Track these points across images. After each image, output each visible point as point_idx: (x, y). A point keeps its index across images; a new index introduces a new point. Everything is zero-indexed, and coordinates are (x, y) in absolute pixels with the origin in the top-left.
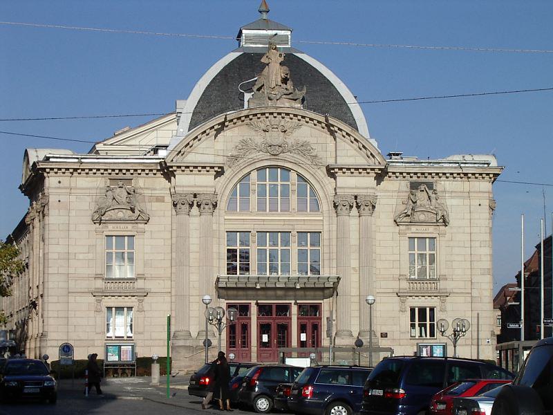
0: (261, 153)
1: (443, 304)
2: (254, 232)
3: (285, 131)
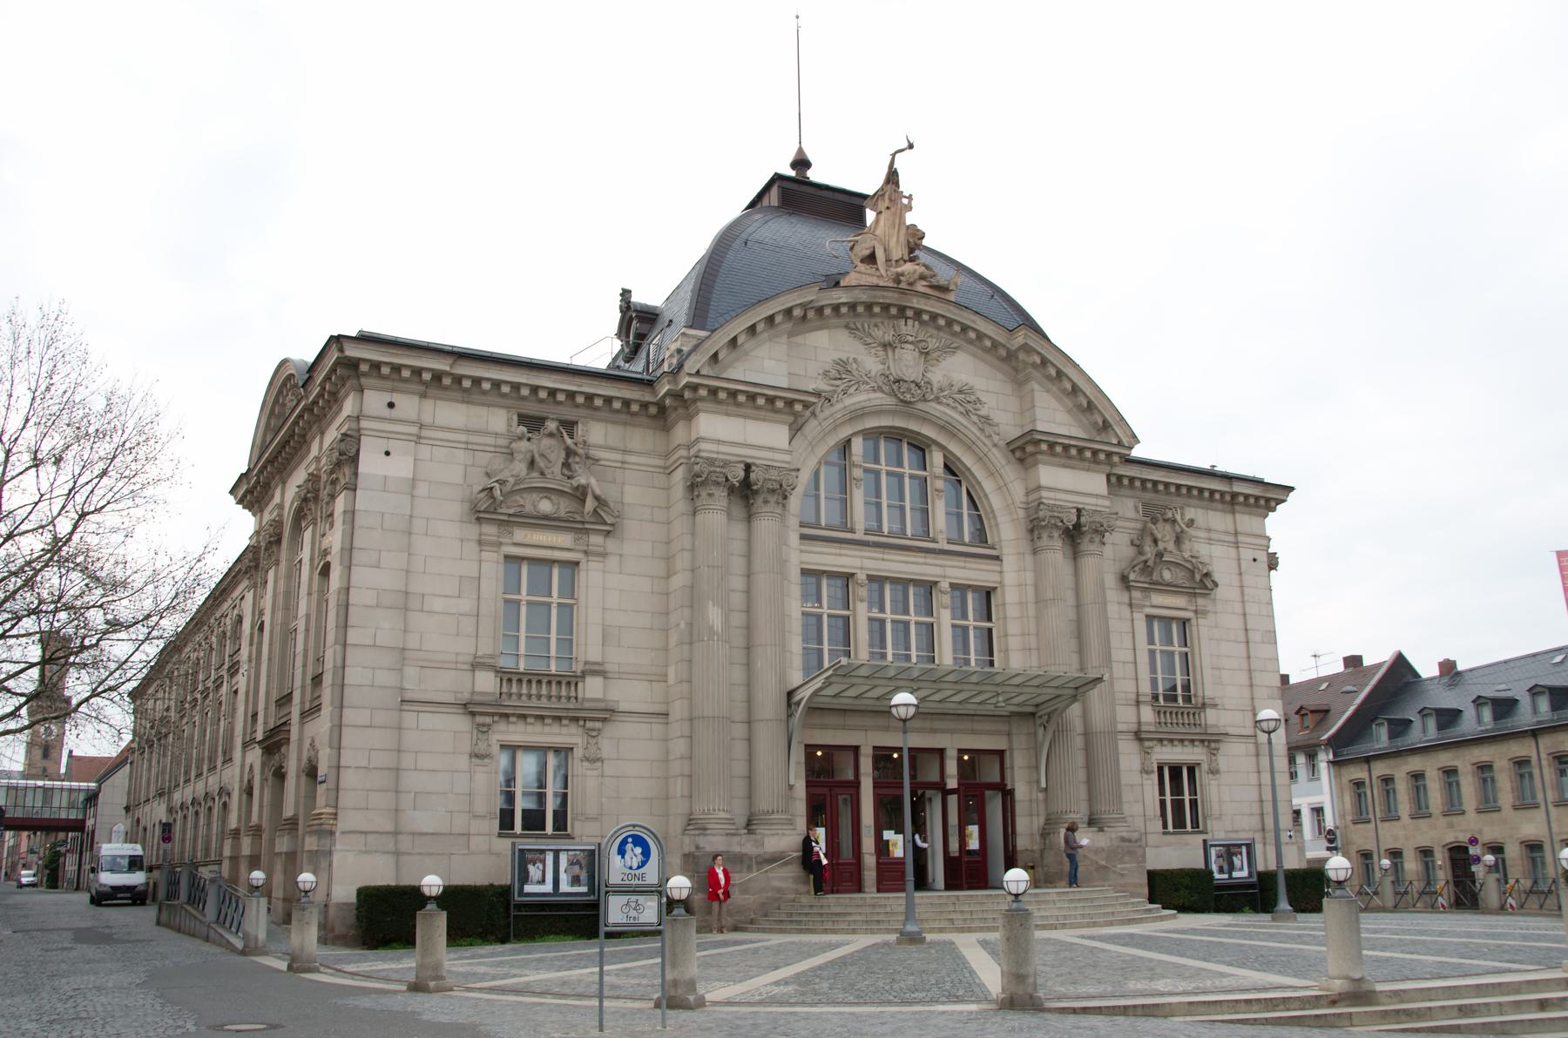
1: (1213, 758)
2: (861, 577)
3: (927, 353)
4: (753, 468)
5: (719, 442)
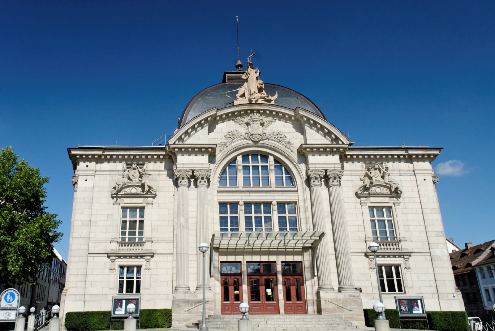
0: (245, 140)
2: (241, 203)
4: (195, 171)
5: (183, 164)
